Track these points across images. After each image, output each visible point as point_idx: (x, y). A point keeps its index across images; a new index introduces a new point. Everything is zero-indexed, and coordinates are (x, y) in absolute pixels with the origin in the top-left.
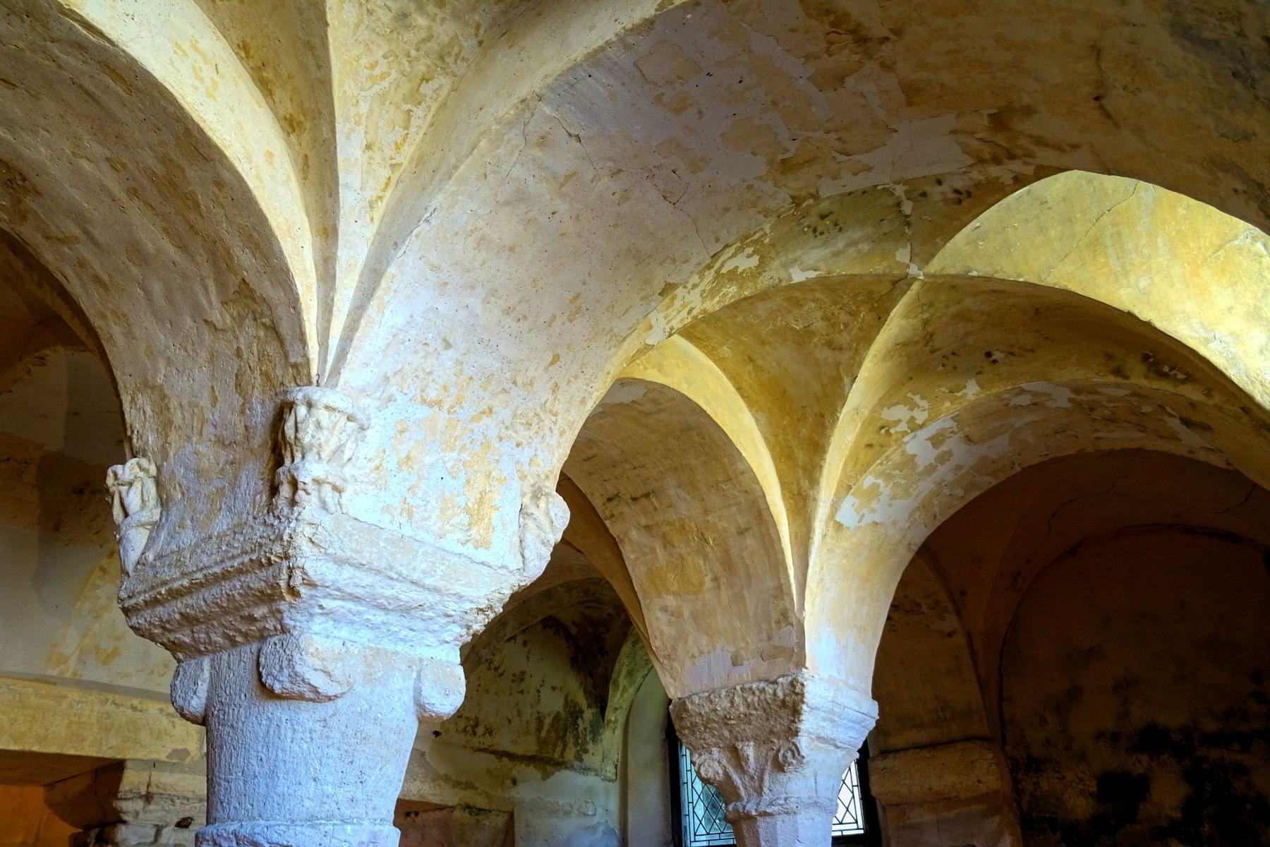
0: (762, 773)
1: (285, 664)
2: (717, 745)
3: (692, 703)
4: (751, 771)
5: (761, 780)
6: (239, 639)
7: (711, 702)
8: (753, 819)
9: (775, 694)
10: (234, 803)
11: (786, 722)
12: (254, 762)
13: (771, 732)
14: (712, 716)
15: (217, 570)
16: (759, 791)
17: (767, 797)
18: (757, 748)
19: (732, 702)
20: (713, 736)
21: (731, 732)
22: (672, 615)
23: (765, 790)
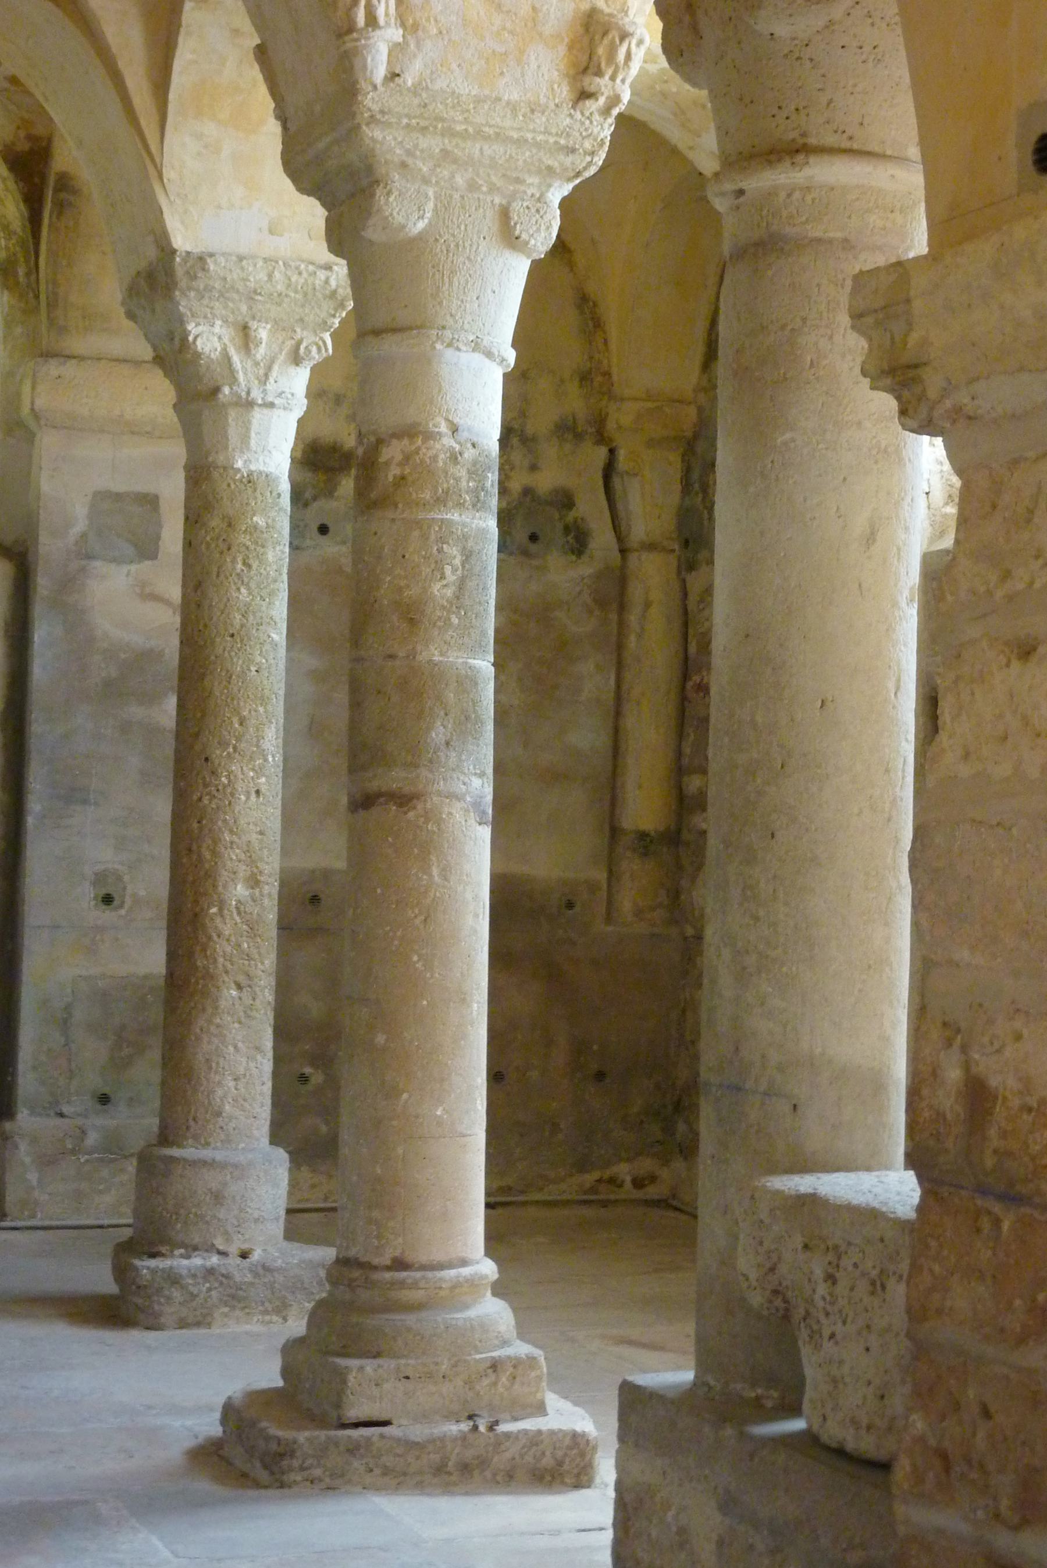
0: (272, 361)
1: (543, 227)
2: (225, 321)
3: (215, 262)
4: (259, 357)
5: (269, 368)
6: (484, 189)
7: (242, 269)
8: (250, 404)
9: (327, 281)
10: (469, 318)
11: (323, 315)
12: (489, 291)
13: (301, 320)
14: (240, 286)
15: (515, 135)
16: (264, 380)
17: (271, 386)
18: (272, 333)
19: (270, 276)
20: (226, 307)
21: (250, 308)
22: (206, 147)
23: (271, 380)
